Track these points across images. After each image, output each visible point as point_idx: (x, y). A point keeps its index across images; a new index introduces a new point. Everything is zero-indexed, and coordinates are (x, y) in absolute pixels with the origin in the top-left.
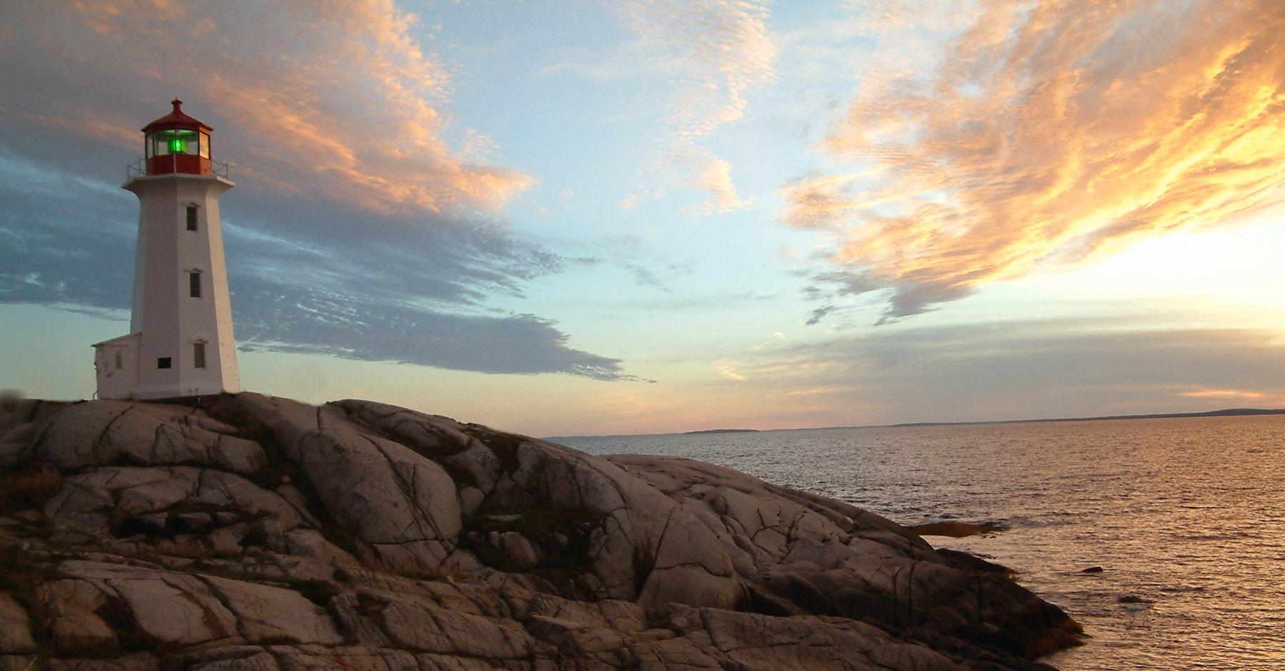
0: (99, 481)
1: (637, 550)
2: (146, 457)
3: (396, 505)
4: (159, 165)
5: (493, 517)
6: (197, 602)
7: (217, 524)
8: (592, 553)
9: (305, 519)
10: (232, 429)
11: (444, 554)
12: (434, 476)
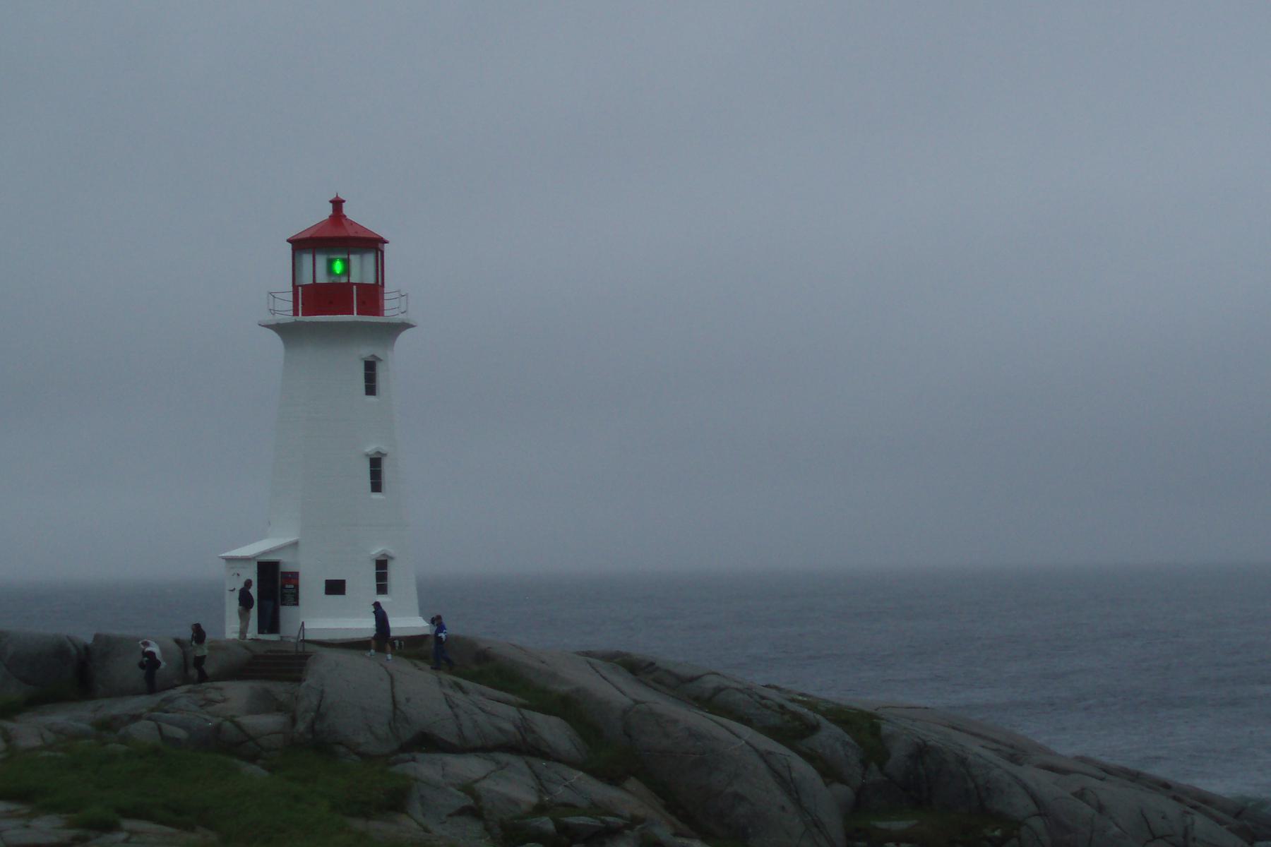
2: (454, 740)
3: (783, 808)
4: (318, 299)
5: (882, 825)
12: (802, 769)
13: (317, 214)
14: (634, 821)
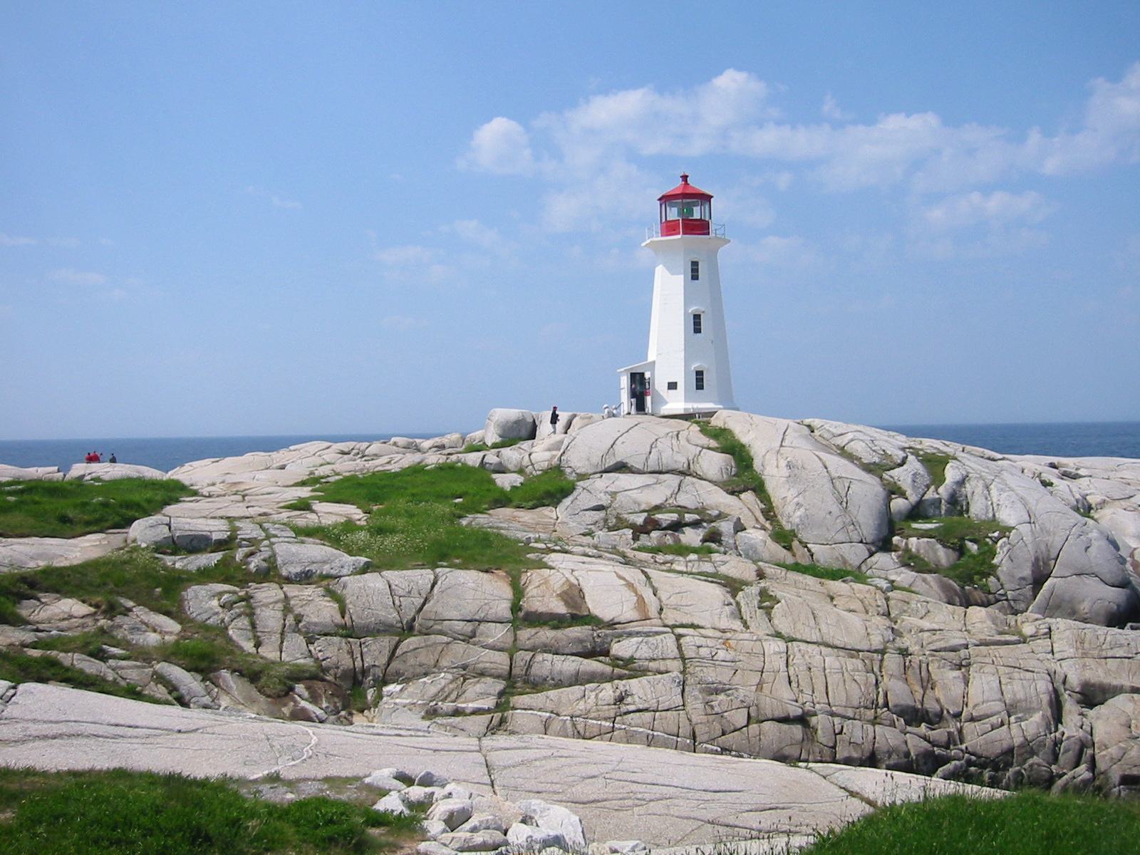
0: (601, 486)
1: (1037, 559)
2: (639, 466)
6: (635, 591)
7: (677, 526)
8: (995, 561)
9: (757, 520)
10: (713, 443)
11: (867, 554)
13: (675, 185)
14: (721, 516)
